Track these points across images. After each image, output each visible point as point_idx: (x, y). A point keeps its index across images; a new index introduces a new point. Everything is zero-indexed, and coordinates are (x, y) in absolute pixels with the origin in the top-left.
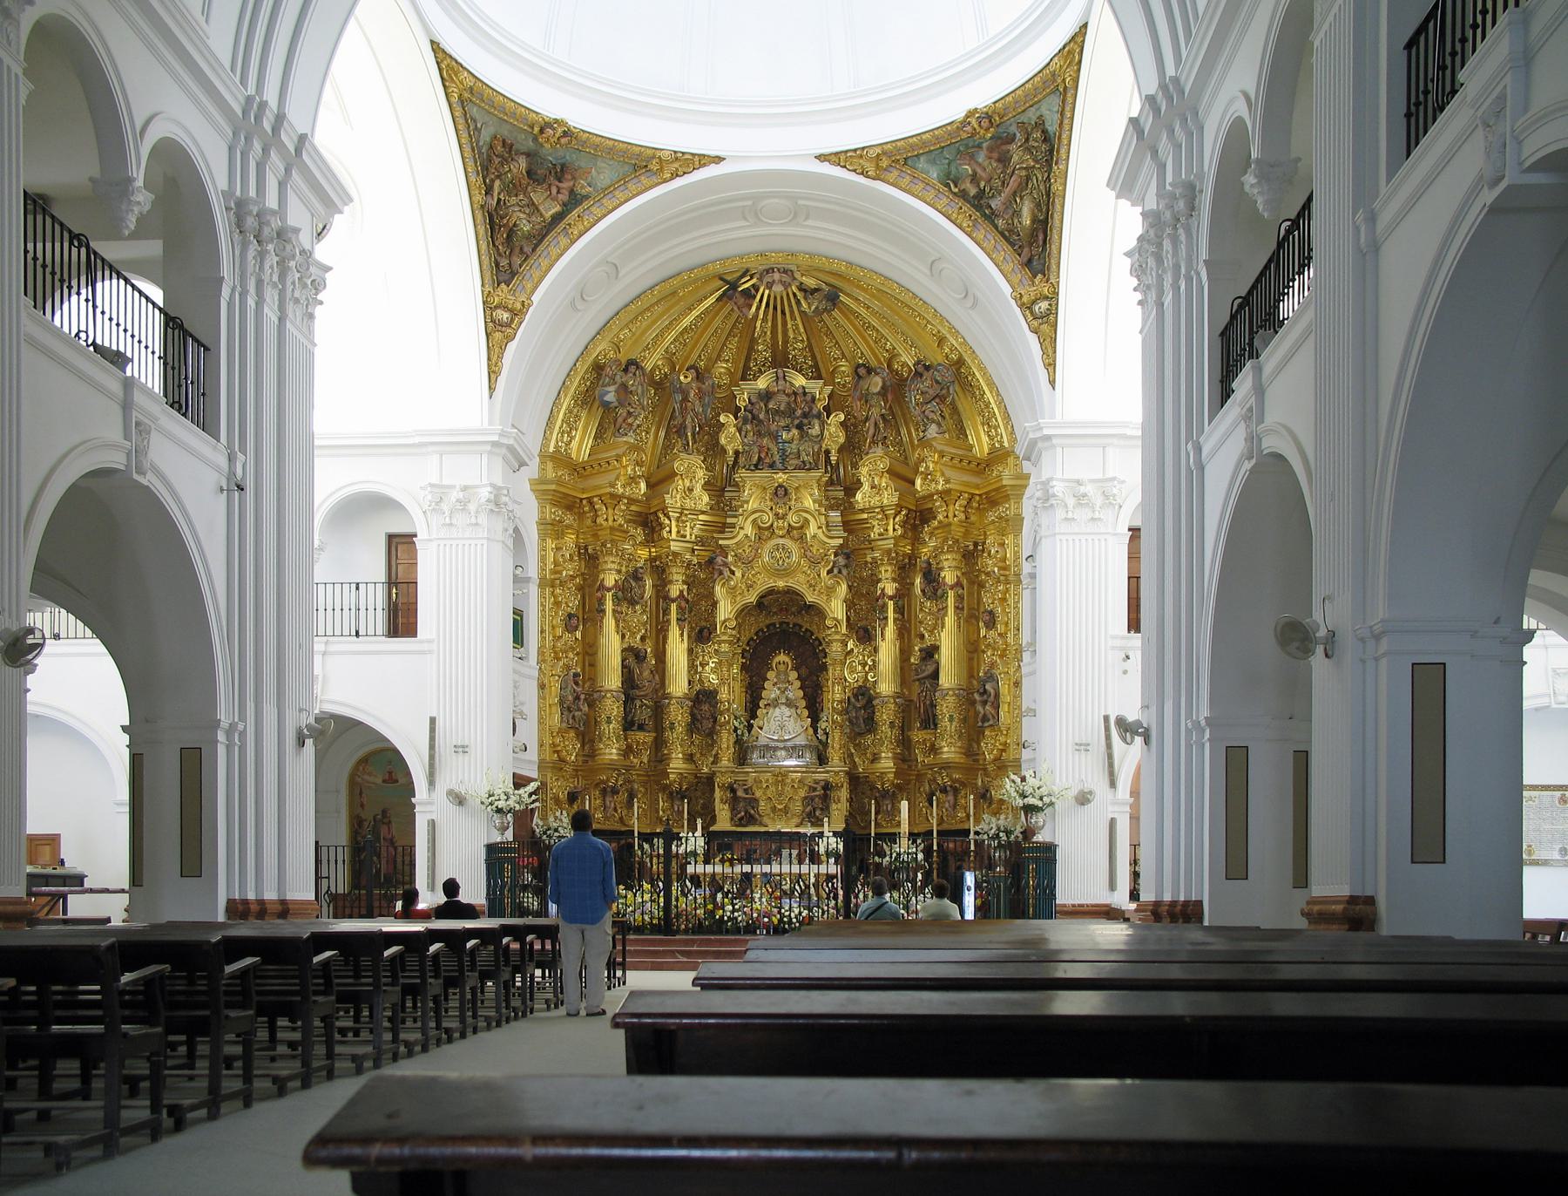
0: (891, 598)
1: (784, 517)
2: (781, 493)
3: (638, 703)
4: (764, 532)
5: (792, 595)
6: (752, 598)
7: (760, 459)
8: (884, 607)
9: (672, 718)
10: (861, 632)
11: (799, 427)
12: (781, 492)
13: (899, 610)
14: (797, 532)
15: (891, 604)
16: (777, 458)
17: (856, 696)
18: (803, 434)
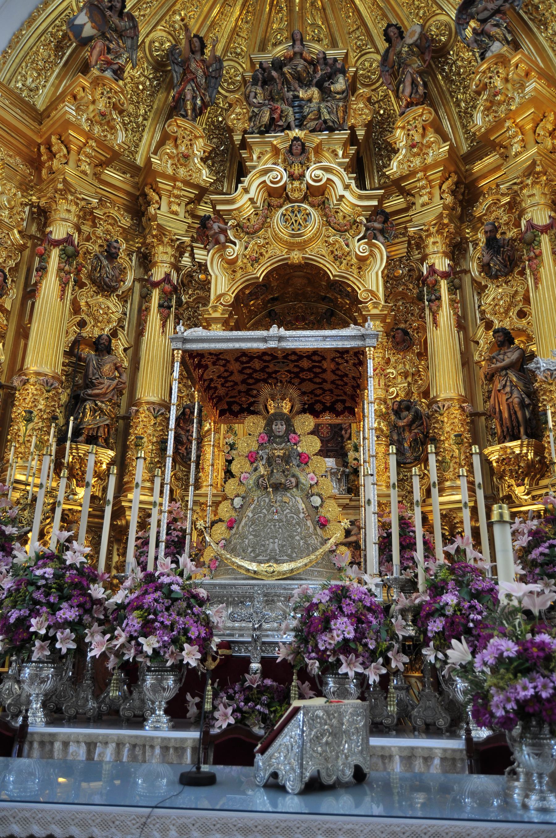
0: (445, 275)
1: (302, 176)
2: (298, 153)
3: (89, 405)
4: (276, 196)
5: (311, 272)
6: (260, 272)
7: (272, 120)
8: (434, 288)
9: (139, 430)
10: (400, 335)
11: (320, 85)
12: (297, 149)
13: (454, 289)
14: (317, 195)
15: (444, 285)
16: (291, 119)
17: (397, 413)
18: (326, 94)
